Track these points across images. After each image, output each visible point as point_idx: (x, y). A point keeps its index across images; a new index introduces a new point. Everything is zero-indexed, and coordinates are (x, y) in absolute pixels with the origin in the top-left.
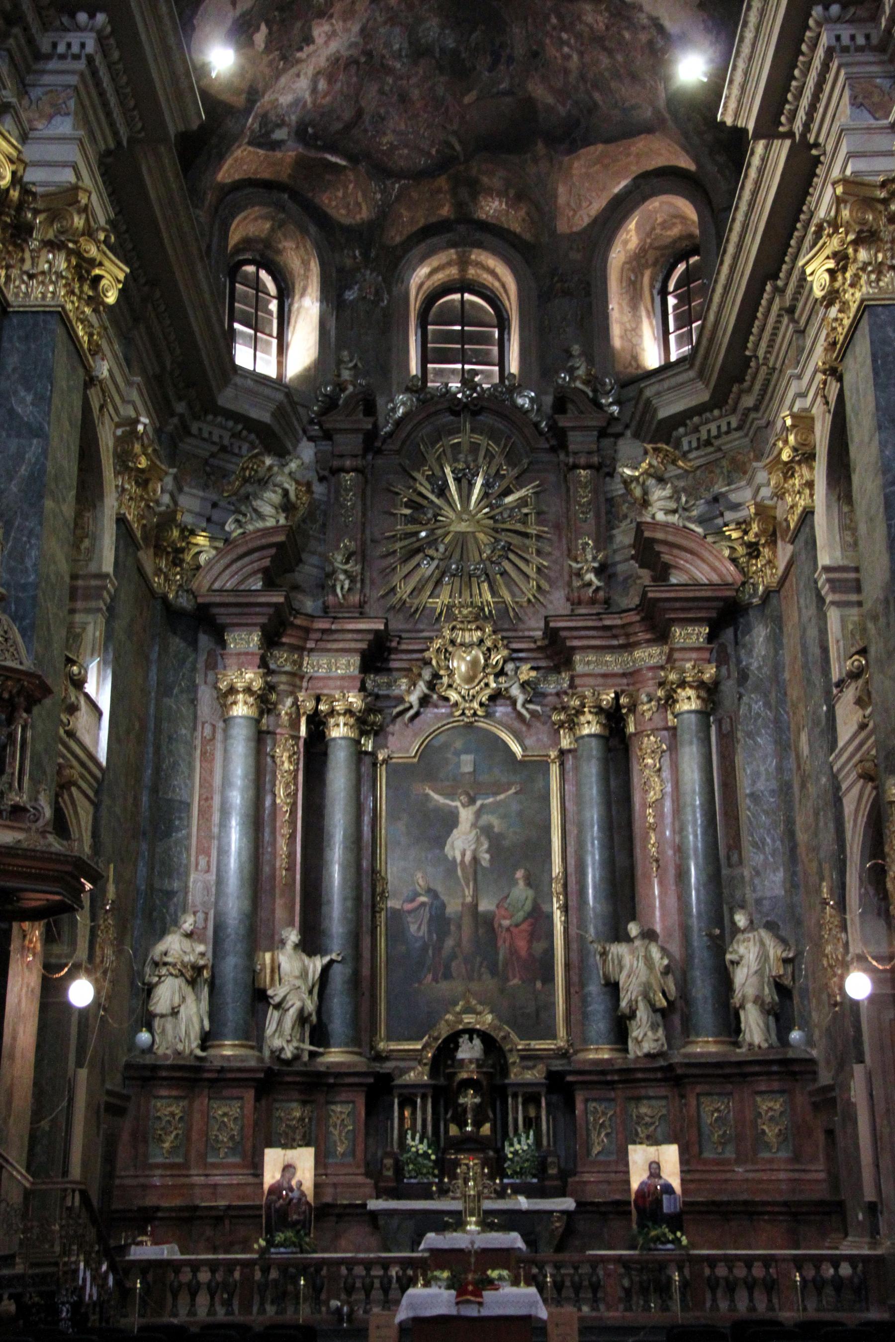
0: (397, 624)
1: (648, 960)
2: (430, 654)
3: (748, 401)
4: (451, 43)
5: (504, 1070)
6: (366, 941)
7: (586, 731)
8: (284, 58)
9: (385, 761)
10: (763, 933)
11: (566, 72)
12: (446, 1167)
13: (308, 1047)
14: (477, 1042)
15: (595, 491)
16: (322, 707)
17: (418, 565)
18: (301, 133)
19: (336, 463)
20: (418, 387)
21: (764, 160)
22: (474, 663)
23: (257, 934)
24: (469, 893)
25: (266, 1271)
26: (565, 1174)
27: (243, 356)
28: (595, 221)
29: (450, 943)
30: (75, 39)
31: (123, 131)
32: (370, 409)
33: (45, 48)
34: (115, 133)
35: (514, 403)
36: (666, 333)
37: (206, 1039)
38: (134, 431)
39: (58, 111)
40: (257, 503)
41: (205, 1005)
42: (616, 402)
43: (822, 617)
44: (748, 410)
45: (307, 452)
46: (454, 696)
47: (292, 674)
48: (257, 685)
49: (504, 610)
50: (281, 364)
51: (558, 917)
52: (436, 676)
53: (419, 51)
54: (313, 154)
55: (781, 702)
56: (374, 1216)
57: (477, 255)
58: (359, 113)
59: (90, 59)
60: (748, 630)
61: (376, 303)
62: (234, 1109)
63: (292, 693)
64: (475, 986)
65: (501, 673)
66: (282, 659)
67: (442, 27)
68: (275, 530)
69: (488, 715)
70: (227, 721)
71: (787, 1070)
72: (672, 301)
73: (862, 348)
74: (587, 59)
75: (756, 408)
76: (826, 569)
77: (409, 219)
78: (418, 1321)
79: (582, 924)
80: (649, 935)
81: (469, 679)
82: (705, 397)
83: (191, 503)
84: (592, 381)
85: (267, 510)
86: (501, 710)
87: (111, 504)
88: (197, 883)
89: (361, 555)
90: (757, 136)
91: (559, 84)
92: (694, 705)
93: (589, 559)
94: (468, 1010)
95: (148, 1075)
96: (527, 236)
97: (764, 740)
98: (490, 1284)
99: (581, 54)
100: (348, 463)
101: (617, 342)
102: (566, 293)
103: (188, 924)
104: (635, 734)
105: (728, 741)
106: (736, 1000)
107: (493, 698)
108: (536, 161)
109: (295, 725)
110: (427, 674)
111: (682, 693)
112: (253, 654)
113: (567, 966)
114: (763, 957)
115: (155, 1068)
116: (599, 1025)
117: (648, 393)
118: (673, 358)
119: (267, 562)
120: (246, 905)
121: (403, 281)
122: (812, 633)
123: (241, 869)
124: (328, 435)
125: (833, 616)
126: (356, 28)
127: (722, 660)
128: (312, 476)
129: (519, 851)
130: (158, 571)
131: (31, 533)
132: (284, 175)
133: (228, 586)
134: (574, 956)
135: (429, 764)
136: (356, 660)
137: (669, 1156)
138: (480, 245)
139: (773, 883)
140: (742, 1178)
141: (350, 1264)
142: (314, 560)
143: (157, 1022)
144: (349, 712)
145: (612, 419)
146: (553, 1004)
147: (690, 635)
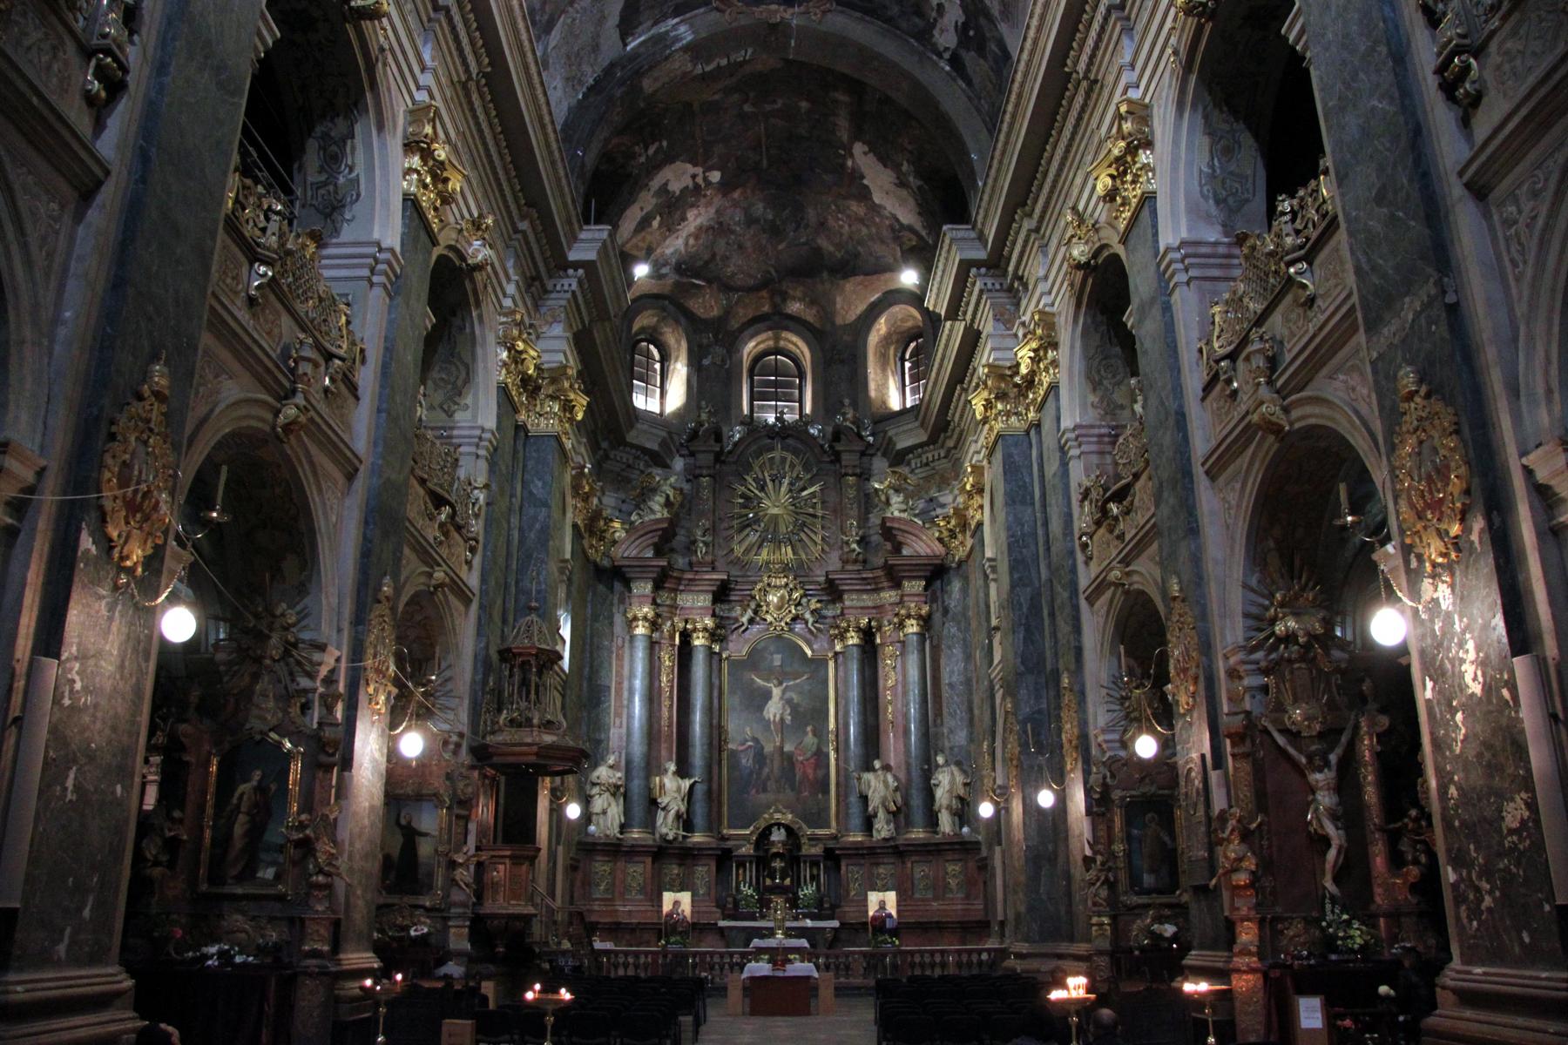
0: (735, 572)
1: (885, 782)
3: (950, 443)
5: (799, 848)
6: (715, 768)
10: (954, 768)
12: (764, 903)
15: (858, 491)
18: (678, 268)
19: (698, 472)
20: (749, 422)
21: (951, 331)
22: (782, 597)
23: (652, 766)
24: (778, 740)
25: (665, 956)
26: (833, 907)
27: (639, 401)
28: (859, 317)
29: (766, 770)
30: (566, 282)
32: (718, 437)
33: (550, 287)
34: (583, 322)
36: (904, 385)
38: (582, 473)
39: (555, 320)
41: (621, 807)
43: (987, 587)
44: (949, 450)
45: (679, 464)
46: (769, 619)
47: (671, 606)
48: (650, 615)
49: (801, 564)
50: (662, 404)
51: (832, 755)
52: (759, 606)
53: (750, 221)
54: (685, 280)
55: (967, 629)
56: (722, 929)
57: (785, 334)
58: (714, 255)
60: (949, 583)
61: (721, 366)
62: (639, 868)
63: (671, 618)
65: (799, 604)
66: (664, 597)
69: (791, 630)
70: (632, 637)
71: (963, 848)
72: (908, 365)
73: (999, 455)
75: (955, 447)
76: (989, 560)
77: (743, 314)
78: (752, 979)
79: (846, 761)
80: (887, 768)
81: (779, 608)
82: (924, 438)
83: (610, 500)
84: (857, 422)
85: (657, 507)
86: (798, 627)
87: (569, 515)
88: (615, 735)
89: (713, 530)
90: (947, 319)
92: (915, 629)
93: (853, 537)
96: (817, 325)
97: (957, 651)
98: (790, 961)
101: (873, 394)
102: (842, 362)
103: (611, 762)
104: (882, 644)
105: (936, 649)
106: (936, 807)
107: (794, 619)
108: (822, 283)
109: (672, 638)
110: (753, 605)
111: (908, 622)
113: (838, 784)
114: (952, 782)
115: (595, 844)
116: (856, 820)
117: (890, 434)
118: (908, 405)
120: (645, 749)
121: (739, 351)
122: (982, 595)
123: (641, 727)
124: (692, 454)
125: (993, 586)
126: (712, 210)
127: (932, 600)
129: (810, 714)
130: (592, 546)
131: (543, 562)
132: (667, 291)
134: (842, 779)
135: (754, 661)
136: (709, 597)
137: (891, 898)
138: (787, 329)
139: (961, 737)
140: (936, 909)
141: (712, 954)
142: (683, 532)
143: (594, 818)
145: (869, 445)
146: (828, 808)
147: (915, 586)
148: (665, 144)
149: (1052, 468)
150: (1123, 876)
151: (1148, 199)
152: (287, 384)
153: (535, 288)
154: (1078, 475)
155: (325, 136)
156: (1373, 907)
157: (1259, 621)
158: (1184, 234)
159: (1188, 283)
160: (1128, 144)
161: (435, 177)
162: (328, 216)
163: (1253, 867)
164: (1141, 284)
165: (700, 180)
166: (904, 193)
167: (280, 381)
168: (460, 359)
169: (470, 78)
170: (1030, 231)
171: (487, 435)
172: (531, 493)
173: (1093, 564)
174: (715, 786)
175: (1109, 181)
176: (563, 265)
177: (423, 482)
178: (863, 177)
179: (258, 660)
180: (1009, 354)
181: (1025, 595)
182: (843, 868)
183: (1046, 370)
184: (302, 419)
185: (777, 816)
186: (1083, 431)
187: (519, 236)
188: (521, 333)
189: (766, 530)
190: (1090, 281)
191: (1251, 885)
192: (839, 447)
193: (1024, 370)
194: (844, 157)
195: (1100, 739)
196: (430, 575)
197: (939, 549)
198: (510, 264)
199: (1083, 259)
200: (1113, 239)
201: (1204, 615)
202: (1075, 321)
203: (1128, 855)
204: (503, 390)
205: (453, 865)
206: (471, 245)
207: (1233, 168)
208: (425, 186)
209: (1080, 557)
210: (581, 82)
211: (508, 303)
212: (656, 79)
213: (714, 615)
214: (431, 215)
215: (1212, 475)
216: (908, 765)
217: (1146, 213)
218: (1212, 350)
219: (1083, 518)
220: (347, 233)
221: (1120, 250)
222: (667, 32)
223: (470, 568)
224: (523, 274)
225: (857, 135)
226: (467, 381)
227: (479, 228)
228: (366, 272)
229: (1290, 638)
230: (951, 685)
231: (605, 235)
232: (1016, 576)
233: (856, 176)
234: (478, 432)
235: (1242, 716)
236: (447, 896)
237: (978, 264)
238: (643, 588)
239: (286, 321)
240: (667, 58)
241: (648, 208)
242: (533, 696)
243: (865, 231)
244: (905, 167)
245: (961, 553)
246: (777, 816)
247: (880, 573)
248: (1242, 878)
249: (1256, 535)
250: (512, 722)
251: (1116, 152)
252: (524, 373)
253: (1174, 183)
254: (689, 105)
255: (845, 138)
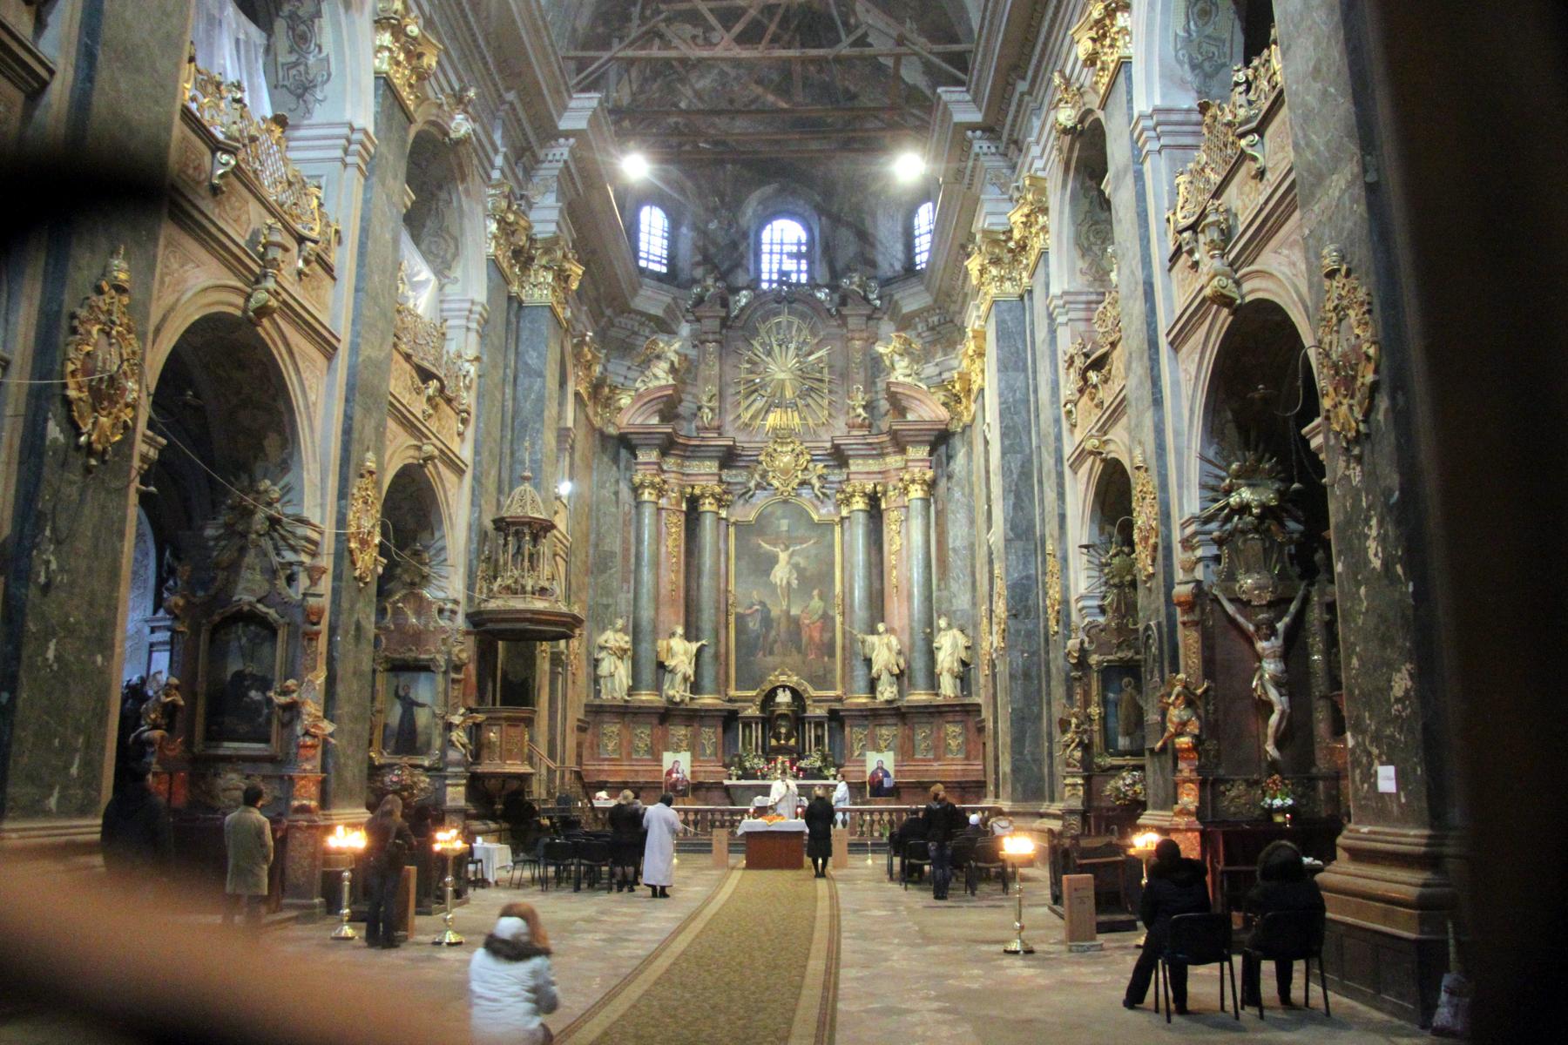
0: (741, 438)
2: (761, 458)
5: (804, 711)
7: (855, 507)
9: (734, 524)
13: (688, 694)
14: (788, 692)
16: (697, 491)
24: (784, 604)
29: (773, 633)
30: (557, 151)
32: (725, 304)
33: (542, 157)
34: (577, 190)
35: (812, 295)
37: (632, 690)
40: (656, 370)
42: (880, 298)
45: (685, 329)
46: (776, 483)
52: (766, 472)
56: (727, 788)
64: (788, 660)
66: (670, 463)
70: (639, 505)
85: (661, 374)
86: (805, 492)
92: (920, 494)
93: (859, 399)
94: (782, 674)
95: (597, 712)
100: (711, 337)
105: (940, 514)
106: (937, 671)
111: (912, 488)
113: (844, 648)
114: (954, 645)
116: (861, 683)
117: (896, 297)
124: (698, 320)
127: (939, 465)
129: (816, 579)
133: (639, 421)
135: (759, 527)
139: (962, 601)
142: (689, 398)
143: (602, 681)
144: (713, 495)
145: (876, 309)
146: (832, 671)
147: (919, 453)
149: (1041, 334)
150: (1097, 739)
151: (1124, 64)
152: (257, 270)
153: (525, 157)
154: (1067, 343)
155: (293, 17)
156: (1314, 770)
157: (1213, 490)
158: (1158, 102)
159: (1159, 152)
160: (1106, 7)
161: (408, 53)
162: (299, 97)
163: (1197, 731)
164: (1117, 152)
167: (253, 265)
170: (1022, 94)
171: (478, 308)
172: (526, 364)
173: (1077, 431)
174: (723, 650)
175: (1090, 45)
177: (408, 357)
179: (244, 535)
180: (1003, 219)
181: (1016, 462)
182: (847, 730)
183: (1037, 234)
184: (273, 303)
185: (783, 678)
186: (1071, 298)
187: (506, 107)
188: (509, 207)
190: (1077, 146)
191: (1195, 748)
192: (845, 311)
193: (1017, 235)
195: (1080, 605)
196: (419, 448)
197: (943, 414)
198: (498, 137)
199: (1070, 124)
200: (1093, 101)
201: (1164, 486)
202: (1064, 186)
203: (1104, 719)
204: (493, 263)
205: (449, 727)
206: (452, 118)
207: (1209, 30)
208: (398, 63)
209: (1065, 425)
213: (721, 481)
214: (405, 93)
215: (1175, 345)
216: (912, 628)
217: (1121, 78)
218: (1176, 222)
219: (1069, 384)
220: (320, 114)
221: (1100, 114)
223: (463, 440)
224: (513, 147)
226: (456, 255)
228: (339, 153)
229: (1244, 508)
230: (954, 550)
231: (595, 103)
232: (1007, 443)
234: (467, 305)
235: (1191, 585)
236: (444, 754)
237: (973, 127)
238: (647, 456)
239: (254, 207)
242: (526, 564)
245: (966, 419)
246: (783, 678)
247: (885, 438)
248: (1184, 741)
249: (1213, 407)
250: (508, 588)
251: (1096, 15)
253: (1149, 46)
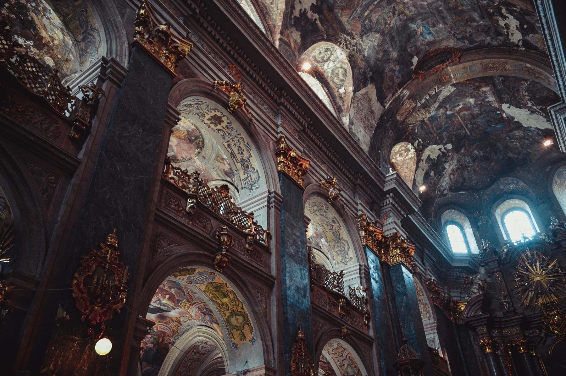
0: (528, 313)
2: (543, 320)
4: (482, 154)
8: (440, 175)
11: (517, 148)
17: (528, 294)
31: (405, 215)
32: (496, 253)
34: (402, 215)
39: (388, 217)
45: (482, 271)
53: (474, 159)
58: (464, 179)
59: (392, 203)
66: (495, 333)
67: (478, 151)
68: (480, 295)
74: (522, 143)
85: (475, 291)
91: (517, 151)
99: (519, 143)
112: (486, 333)
119: (481, 306)
124: (487, 264)
128: (486, 277)
148: (420, 140)
155: (242, 160)
161: (294, 163)
165: (443, 150)
166: (535, 115)
168: (344, 240)
169: (304, 126)
172: (397, 291)
176: (384, 194)
178: (513, 118)
189: (536, 289)
194: (501, 114)
206: (329, 191)
208: (289, 167)
210: (371, 127)
211: (360, 213)
212: (402, 115)
213: (525, 337)
214: (295, 178)
222: (399, 96)
223: (369, 327)
225: (501, 101)
227: (331, 184)
233: (511, 119)
240: (403, 104)
241: (426, 169)
243: (527, 142)
244: (530, 104)
252: (377, 240)
254: (423, 121)
255: (497, 105)
